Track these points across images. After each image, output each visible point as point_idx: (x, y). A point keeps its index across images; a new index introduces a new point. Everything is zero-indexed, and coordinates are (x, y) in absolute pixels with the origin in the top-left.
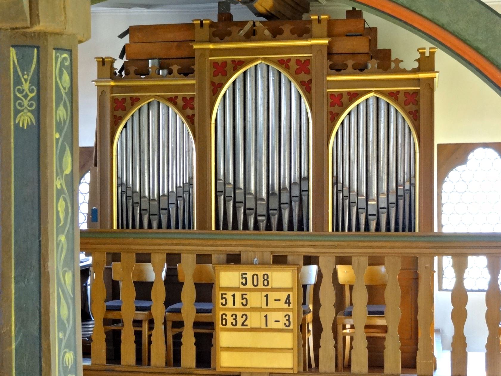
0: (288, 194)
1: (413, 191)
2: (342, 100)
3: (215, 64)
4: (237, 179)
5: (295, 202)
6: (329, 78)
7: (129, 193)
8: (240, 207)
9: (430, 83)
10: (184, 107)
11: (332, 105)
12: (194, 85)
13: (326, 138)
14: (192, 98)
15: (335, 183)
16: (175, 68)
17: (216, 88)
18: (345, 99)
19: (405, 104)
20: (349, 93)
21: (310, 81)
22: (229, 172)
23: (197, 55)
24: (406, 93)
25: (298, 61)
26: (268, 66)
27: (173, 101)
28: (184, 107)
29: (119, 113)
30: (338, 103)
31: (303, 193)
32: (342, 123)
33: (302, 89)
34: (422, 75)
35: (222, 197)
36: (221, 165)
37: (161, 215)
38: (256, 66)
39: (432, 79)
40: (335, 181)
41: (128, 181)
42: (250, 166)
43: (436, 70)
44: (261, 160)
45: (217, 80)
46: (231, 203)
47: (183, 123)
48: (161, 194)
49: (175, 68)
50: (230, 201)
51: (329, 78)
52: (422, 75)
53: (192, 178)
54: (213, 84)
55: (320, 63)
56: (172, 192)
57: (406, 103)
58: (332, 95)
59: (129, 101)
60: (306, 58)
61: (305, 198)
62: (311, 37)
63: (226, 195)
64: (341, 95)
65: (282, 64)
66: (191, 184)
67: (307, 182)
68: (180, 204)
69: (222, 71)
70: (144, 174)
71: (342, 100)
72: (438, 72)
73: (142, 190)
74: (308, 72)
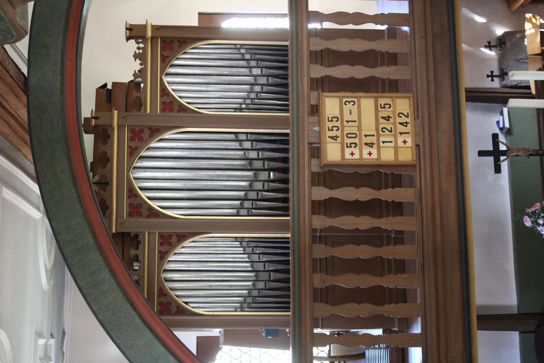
0: (250, 152)
1: (247, 47)
2: (168, 102)
3: (130, 215)
4: (236, 198)
5: (257, 145)
6: (148, 112)
7: (249, 300)
8: (262, 195)
9: (156, 28)
10: (170, 244)
11: (172, 110)
12: (149, 233)
13: (200, 115)
14: (161, 236)
15: (241, 110)
16: (133, 252)
17: (153, 213)
18: (166, 99)
19: (173, 50)
20: (162, 96)
21: (150, 129)
22: (231, 204)
23: (121, 230)
24: (162, 49)
25: (131, 139)
26: (134, 168)
27: (163, 256)
28: (170, 244)
29: (173, 308)
30: (170, 104)
31: (249, 138)
32: (188, 103)
33: (157, 137)
34: (149, 34)
35: (253, 210)
36: (224, 211)
37: (270, 269)
38: (134, 179)
39: (153, 26)
40: (239, 110)
41: (238, 302)
42: (225, 186)
43: (145, 23)
44: (219, 176)
45: (145, 213)
46: (258, 203)
47: (183, 247)
48: (251, 269)
49: (133, 252)
50: (256, 204)
51: (148, 112)
52: (149, 34)
53: (236, 238)
54: (148, 217)
55: (135, 119)
56: (249, 257)
57: (172, 49)
58: (163, 110)
59: (162, 299)
60: (129, 132)
61: (253, 137)
62: (111, 126)
63: (251, 207)
64: (163, 103)
65: (133, 153)
66: (241, 240)
67: (240, 135)
68: (260, 250)
69: (138, 208)
70: (232, 286)
71: (168, 102)
72: (147, 21)
73: (247, 288)
74: (142, 131)
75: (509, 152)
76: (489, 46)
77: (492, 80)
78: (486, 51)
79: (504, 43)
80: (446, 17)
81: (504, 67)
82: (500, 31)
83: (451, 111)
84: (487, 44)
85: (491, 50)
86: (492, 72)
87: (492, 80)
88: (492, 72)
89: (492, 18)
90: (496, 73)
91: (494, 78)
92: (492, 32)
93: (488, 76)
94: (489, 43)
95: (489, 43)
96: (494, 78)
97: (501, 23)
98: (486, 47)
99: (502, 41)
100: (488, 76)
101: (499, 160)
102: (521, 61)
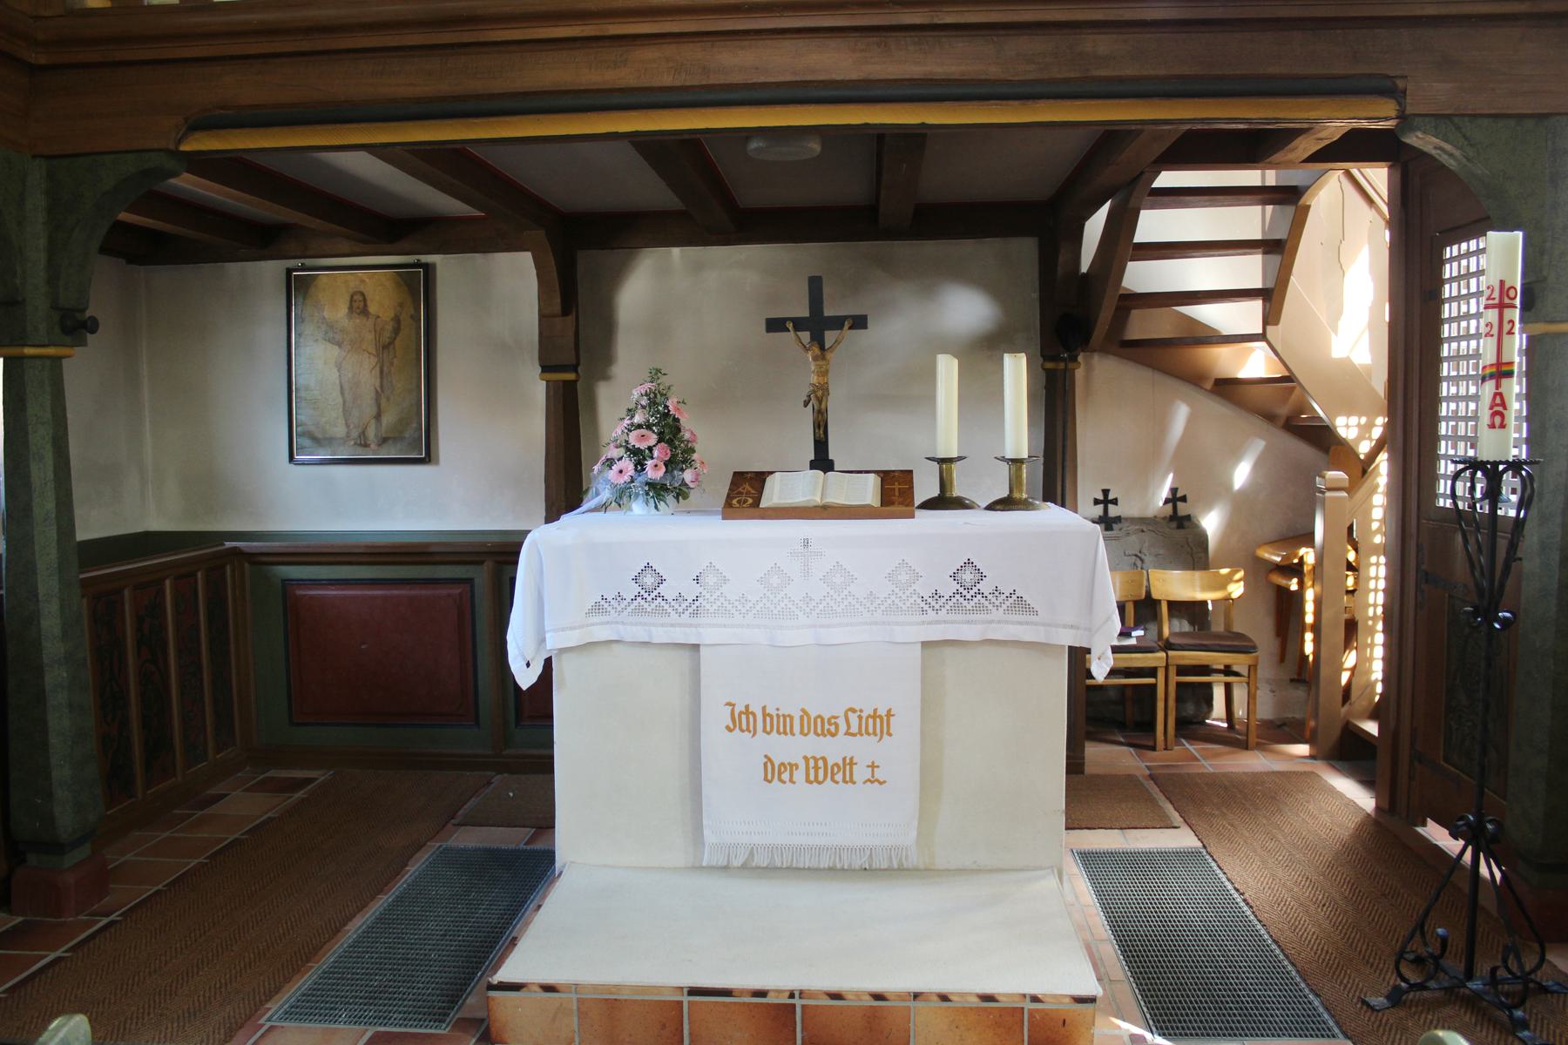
75: (817, 351)
76: (1175, 498)
77: (1097, 502)
78: (1165, 493)
79: (1181, 526)
80: (1129, 71)
81: (1124, 525)
82: (1211, 522)
83: (854, 76)
84: (1179, 494)
85: (1167, 501)
86: (1115, 502)
87: (1097, 502)
88: (1115, 502)
89: (1242, 505)
90: (1113, 511)
91: (1101, 507)
92: (1208, 506)
93: (1106, 492)
94: (1184, 499)
95: (1184, 499)
96: (1101, 507)
97: (1230, 527)
98: (1174, 491)
99: (1186, 524)
100: (1106, 492)
101: (796, 329)
102: (1139, 563)
